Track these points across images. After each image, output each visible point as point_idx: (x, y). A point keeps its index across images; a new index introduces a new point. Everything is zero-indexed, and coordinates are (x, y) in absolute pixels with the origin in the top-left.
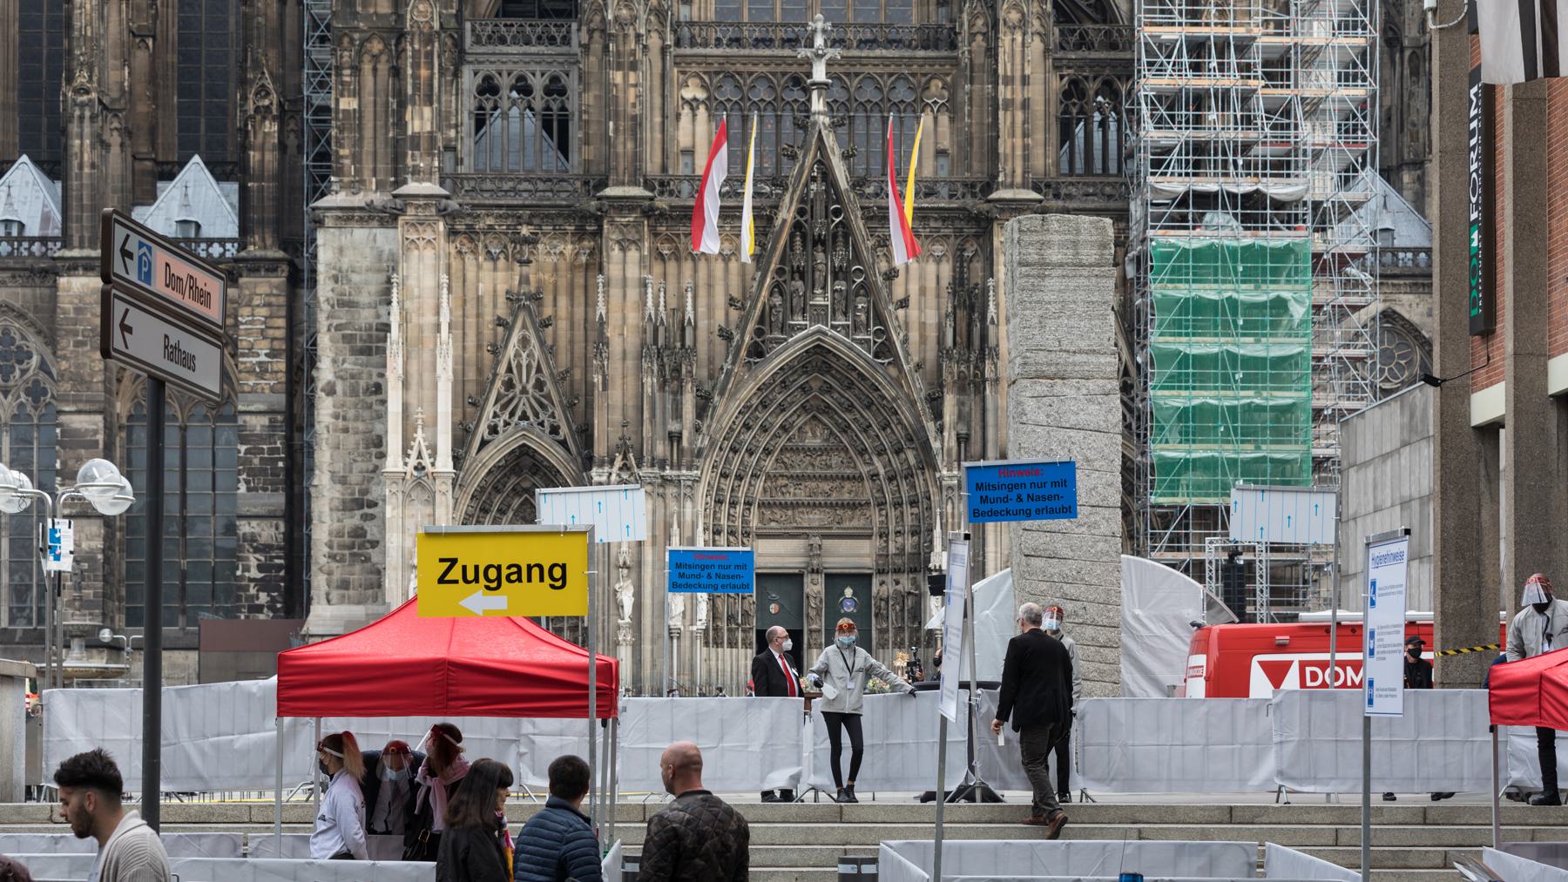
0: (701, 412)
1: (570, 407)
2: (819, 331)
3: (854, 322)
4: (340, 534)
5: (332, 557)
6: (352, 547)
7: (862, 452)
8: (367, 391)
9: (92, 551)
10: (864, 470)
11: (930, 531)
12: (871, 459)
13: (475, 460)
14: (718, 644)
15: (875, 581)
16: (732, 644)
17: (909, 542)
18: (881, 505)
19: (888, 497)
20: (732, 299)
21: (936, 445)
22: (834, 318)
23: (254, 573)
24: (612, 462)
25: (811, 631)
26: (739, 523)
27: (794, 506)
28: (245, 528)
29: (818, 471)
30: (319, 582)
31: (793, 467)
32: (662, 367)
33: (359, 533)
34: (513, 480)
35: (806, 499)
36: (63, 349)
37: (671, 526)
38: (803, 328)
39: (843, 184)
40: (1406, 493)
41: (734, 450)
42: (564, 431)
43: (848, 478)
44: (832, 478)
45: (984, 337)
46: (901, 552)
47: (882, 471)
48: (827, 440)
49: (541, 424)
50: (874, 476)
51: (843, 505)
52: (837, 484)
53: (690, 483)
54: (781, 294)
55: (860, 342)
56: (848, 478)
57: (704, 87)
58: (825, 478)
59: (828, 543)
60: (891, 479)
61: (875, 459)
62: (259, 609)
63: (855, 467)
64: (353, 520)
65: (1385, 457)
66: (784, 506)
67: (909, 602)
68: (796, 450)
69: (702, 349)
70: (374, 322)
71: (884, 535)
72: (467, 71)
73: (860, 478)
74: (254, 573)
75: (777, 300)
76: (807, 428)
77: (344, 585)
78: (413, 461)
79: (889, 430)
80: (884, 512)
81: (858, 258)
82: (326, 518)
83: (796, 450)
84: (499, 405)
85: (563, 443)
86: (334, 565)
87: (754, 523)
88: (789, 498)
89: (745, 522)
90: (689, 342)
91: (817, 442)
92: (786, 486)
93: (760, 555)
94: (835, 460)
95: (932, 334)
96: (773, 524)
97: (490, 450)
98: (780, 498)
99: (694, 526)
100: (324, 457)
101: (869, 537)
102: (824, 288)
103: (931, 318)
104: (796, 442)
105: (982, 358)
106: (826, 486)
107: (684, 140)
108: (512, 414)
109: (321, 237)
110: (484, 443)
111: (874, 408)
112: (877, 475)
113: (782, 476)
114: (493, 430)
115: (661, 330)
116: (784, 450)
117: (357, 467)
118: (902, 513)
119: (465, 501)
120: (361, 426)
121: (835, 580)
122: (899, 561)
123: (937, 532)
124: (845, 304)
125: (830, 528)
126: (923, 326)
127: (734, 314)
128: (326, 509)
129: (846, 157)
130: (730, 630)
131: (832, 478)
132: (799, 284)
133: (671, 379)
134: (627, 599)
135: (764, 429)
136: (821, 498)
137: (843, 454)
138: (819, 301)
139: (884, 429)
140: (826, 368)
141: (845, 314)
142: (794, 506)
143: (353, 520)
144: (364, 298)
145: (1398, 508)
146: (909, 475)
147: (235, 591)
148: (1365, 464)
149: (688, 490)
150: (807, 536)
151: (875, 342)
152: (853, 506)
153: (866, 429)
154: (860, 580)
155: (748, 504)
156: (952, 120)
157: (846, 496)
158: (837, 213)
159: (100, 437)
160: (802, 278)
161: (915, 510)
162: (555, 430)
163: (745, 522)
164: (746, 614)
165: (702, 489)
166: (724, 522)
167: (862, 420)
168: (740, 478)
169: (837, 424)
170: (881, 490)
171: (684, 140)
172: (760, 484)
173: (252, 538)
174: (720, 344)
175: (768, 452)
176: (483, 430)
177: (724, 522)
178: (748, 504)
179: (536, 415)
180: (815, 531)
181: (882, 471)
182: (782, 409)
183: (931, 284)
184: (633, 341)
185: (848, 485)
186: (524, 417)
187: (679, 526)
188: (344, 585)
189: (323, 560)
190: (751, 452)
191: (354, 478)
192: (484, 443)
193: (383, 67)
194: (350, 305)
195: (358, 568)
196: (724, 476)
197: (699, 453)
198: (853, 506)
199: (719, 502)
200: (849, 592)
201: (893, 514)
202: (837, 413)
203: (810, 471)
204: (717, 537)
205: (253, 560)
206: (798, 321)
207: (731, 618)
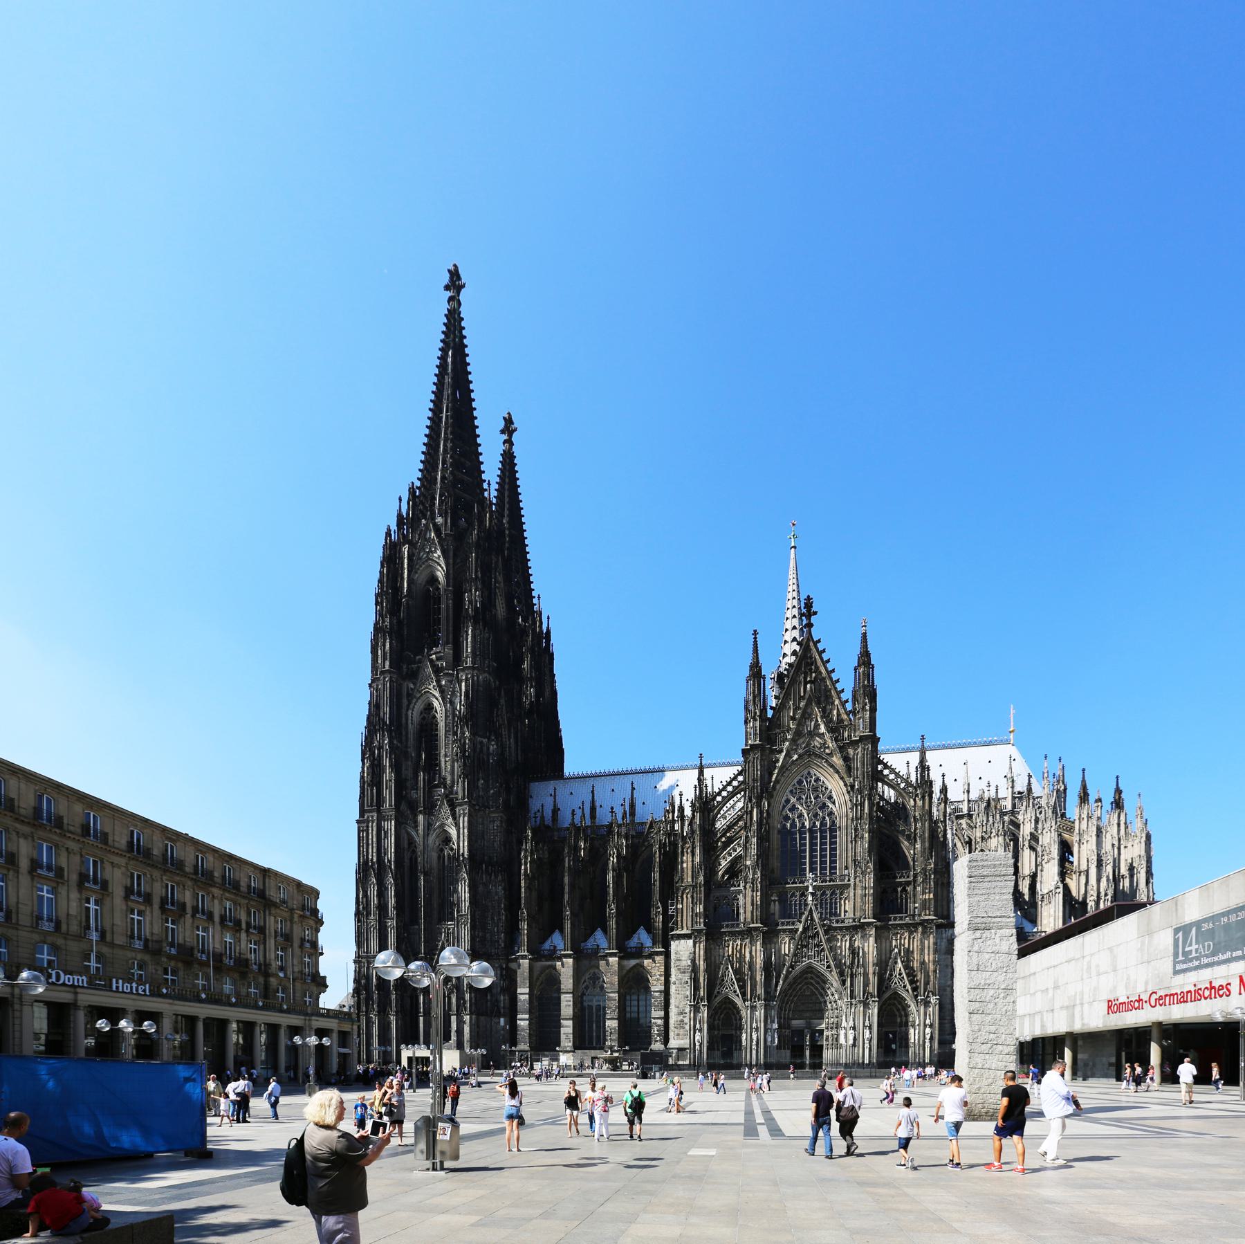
8: (684, 983)
14: (780, 1049)
15: (825, 1030)
16: (784, 1049)
27: (803, 1011)
30: (671, 1034)
41: (786, 996)
51: (816, 1011)
57: (777, 896)
64: (681, 1017)
66: (799, 1011)
67: (835, 1036)
72: (712, 895)
77: (678, 1035)
85: (738, 995)
100: (673, 1001)
107: (772, 911)
109: (672, 943)
134: (754, 1037)
144: (683, 959)
162: (735, 992)
171: (772, 911)
176: (716, 992)
178: (789, 1010)
182: (799, 984)
188: (678, 1035)
190: (790, 996)
192: (716, 997)
193: (689, 896)
194: (680, 960)
206: (804, 959)
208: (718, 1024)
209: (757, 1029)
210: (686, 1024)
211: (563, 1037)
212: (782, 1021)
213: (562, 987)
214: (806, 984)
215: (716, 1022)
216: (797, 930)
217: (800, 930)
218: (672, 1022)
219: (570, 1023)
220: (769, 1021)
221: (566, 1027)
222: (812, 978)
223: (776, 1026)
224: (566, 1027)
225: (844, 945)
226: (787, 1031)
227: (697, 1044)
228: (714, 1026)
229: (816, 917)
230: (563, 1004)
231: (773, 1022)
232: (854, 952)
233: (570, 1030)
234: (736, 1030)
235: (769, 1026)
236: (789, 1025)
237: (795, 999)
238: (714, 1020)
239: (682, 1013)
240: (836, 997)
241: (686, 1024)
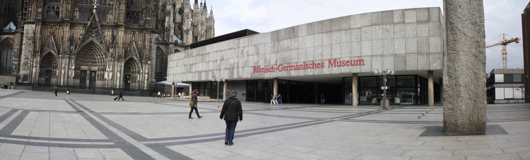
1: (57, 47)
2: (93, 39)
4: (24, 62)
5: (23, 65)
6: (26, 64)
7: (97, 55)
11: (106, 66)
17: (103, 67)
19: (100, 61)
20: (81, 34)
21: (108, 55)
23: (14, 68)
24: (62, 54)
27: (87, 62)
28: (13, 62)
29: (90, 58)
30: (21, 68)
32: (70, 42)
33: (27, 62)
34: (48, 56)
38: (90, 39)
39: (97, 21)
40: (186, 64)
41: (79, 54)
42: (56, 50)
44: (92, 59)
45: (116, 42)
46: (102, 69)
47: (99, 58)
50: (98, 59)
54: (88, 34)
55: (98, 41)
59: (91, 67)
60: (101, 59)
62: (14, 72)
64: (26, 61)
65: (180, 59)
66: (85, 62)
67: (102, 75)
69: (76, 41)
70: (31, 36)
71: (99, 66)
73: (96, 59)
74: (14, 68)
75: (87, 35)
77: (24, 69)
81: (99, 30)
82: (23, 60)
83: (87, 55)
85: (55, 52)
86: (23, 66)
88: (86, 61)
90: (74, 39)
91: (90, 54)
94: (93, 56)
95: (108, 41)
97: (45, 52)
98: (85, 61)
99: (73, 63)
101: (97, 66)
102: (94, 34)
103: (108, 39)
105: (115, 44)
106: (91, 60)
115: (71, 38)
117: (27, 54)
119: (42, 58)
120: (28, 49)
121: (91, 72)
122: (101, 70)
123: (107, 66)
124: (97, 36)
126: (107, 40)
127: (81, 37)
128: (23, 59)
129: (98, 18)
130: (77, 77)
132: (90, 33)
133: (71, 44)
135: (83, 52)
138: (93, 35)
141: (96, 37)
142: (87, 62)
143: (26, 61)
145: (183, 66)
146: (103, 59)
147: (12, 70)
148: (173, 61)
150: (88, 66)
152: (95, 62)
153: (98, 52)
154: (95, 72)
156: (112, 15)
157: (94, 61)
158: (96, 24)
160: (91, 32)
162: (54, 50)
164: (79, 75)
168: (79, 58)
169: (93, 52)
173: (14, 64)
174: (78, 40)
175: (83, 55)
177: (77, 63)
178: (80, 61)
179: (52, 48)
181: (99, 58)
182: (86, 49)
183: (108, 35)
184: (67, 39)
185: (94, 60)
188: (24, 69)
189: (22, 65)
190: (81, 54)
191: (27, 55)
192: (45, 51)
195: (26, 67)
196: (77, 57)
197: (74, 54)
199: (77, 60)
200: (93, 73)
203: (89, 57)
205: (14, 66)
206: (90, 38)
207: (77, 76)
208: (45, 65)
210: (29, 64)
212: (77, 65)
215: (44, 64)
216: (87, 24)
217: (89, 24)
218: (22, 62)
220: (70, 65)
223: (73, 67)
225: (108, 34)
228: (42, 66)
229: (97, 19)
231: (72, 65)
232: (114, 37)
234: (53, 68)
236: (80, 68)
238: (43, 63)
239: (27, 59)
240: (104, 56)
241: (29, 64)
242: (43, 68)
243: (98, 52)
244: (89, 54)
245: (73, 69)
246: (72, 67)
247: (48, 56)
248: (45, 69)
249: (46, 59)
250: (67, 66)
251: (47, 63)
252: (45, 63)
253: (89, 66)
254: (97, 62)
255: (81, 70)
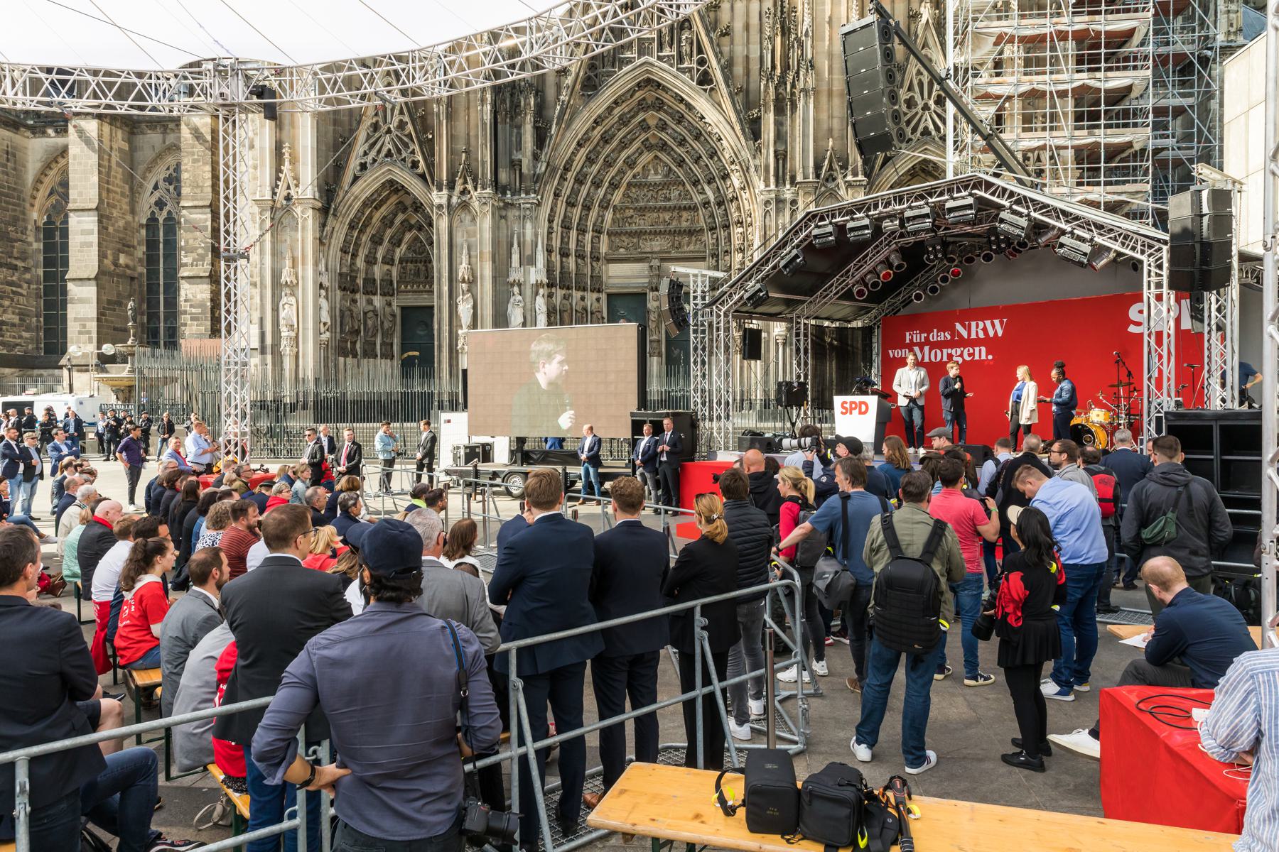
0: (541, 138)
3: (679, 53)
7: (696, 183)
9: (203, 301)
10: (698, 199)
12: (703, 189)
13: (347, 192)
18: (712, 229)
22: (661, 48)
25: (651, 341)
26: (588, 248)
27: (639, 234)
31: (637, 201)
35: (649, 228)
36: (186, 164)
37: (512, 245)
43: (685, 208)
47: (712, 197)
48: (666, 176)
49: (404, 160)
50: (706, 204)
51: (681, 233)
52: (675, 214)
53: (529, 206)
56: (685, 208)
58: (665, 209)
61: (706, 188)
63: (691, 199)
66: (631, 234)
68: (640, 186)
73: (695, 209)
76: (650, 167)
78: (281, 192)
79: (716, 158)
80: (715, 236)
83: (640, 186)
84: (367, 145)
87: (604, 248)
88: (634, 227)
89: (595, 248)
91: (658, 178)
92: (632, 217)
93: (609, 277)
96: (622, 250)
98: (628, 228)
101: (703, 259)
104: (639, 179)
106: (667, 216)
108: (379, 151)
110: (356, 179)
111: (702, 138)
112: (709, 203)
113: (627, 208)
114: (363, 167)
116: (629, 185)
118: (730, 234)
125: (670, 252)
131: (673, 209)
136: (662, 227)
137: (681, 188)
139: (711, 157)
140: (659, 105)
149: (528, 212)
151: (698, 70)
152: (690, 233)
155: (598, 231)
157: (685, 225)
159: (209, 223)
161: (740, 230)
162: (415, 165)
163: (595, 248)
165: (544, 212)
166: (573, 246)
167: (693, 152)
170: (712, 216)
172: (609, 215)
178: (598, 231)
179: (399, 151)
180: (655, 256)
181: (712, 197)
182: (623, 145)
183: (754, 21)
185: (685, 215)
186: (389, 154)
187: (519, 246)
190: (596, 184)
192: (356, 179)
197: (537, 179)
198: (690, 233)
201: (723, 234)
202: (673, 149)
204: (564, 259)
209: (472, 282)
211: (72, 328)
213: (73, 194)
214: (647, 146)
215: (378, 271)
219: (90, 291)
220: (515, 257)
221: (81, 301)
222: (663, 127)
224: (81, 301)
226: (591, 297)
227: (285, 332)
230: (75, 240)
231: (529, 261)
233: (91, 311)
235: (515, 275)
237: (617, 197)
242: (375, 294)
243: (698, 160)
244: (654, 178)
245: (538, 285)
246: (526, 274)
247: (400, 217)
248: (389, 304)
249: (389, 233)
250: (486, 270)
251: (401, 261)
252: (388, 260)
253: (655, 263)
254: (702, 230)
255: (609, 295)
